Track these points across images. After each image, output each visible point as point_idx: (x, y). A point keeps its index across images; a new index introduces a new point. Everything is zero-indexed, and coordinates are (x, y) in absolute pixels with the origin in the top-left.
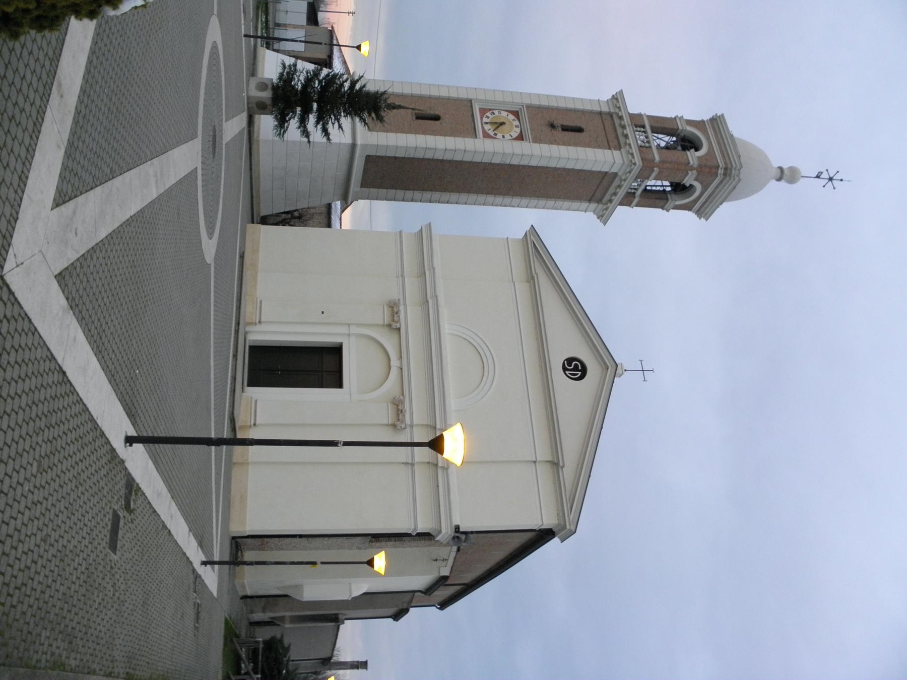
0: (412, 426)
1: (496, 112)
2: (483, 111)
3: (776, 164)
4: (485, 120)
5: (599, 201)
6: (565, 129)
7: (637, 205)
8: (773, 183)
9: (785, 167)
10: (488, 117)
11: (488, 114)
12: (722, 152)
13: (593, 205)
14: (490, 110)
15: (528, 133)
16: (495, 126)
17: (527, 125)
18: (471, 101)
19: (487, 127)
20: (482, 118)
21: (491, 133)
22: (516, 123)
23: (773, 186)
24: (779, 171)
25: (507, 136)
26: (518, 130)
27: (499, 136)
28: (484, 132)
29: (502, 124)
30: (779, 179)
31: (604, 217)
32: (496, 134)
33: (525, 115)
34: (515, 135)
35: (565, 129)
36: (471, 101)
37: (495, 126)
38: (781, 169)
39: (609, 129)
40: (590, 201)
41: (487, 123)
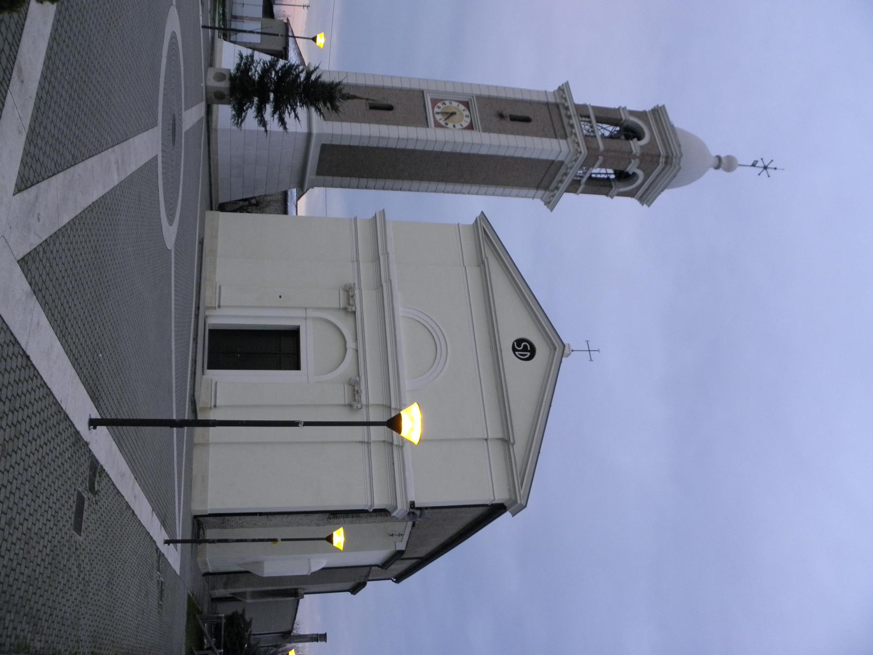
0: (367, 406)
1: (447, 103)
2: (435, 102)
3: (714, 153)
4: (436, 110)
5: (546, 188)
6: (514, 119)
7: (583, 192)
8: (712, 172)
9: (723, 155)
10: (439, 107)
11: (439, 104)
12: (663, 140)
13: (541, 192)
14: (441, 100)
15: (478, 123)
18: (423, 92)
19: (438, 117)
20: (433, 108)
21: (442, 122)
22: (467, 113)
23: (712, 175)
24: (717, 160)
25: (458, 126)
26: (469, 120)
27: (450, 125)
29: (453, 114)
30: (717, 168)
31: (551, 204)
32: (447, 124)
33: (475, 105)
34: (465, 124)
35: (514, 119)
36: (423, 92)
37: (446, 116)
39: (556, 119)
40: (538, 188)
41: (438, 113)
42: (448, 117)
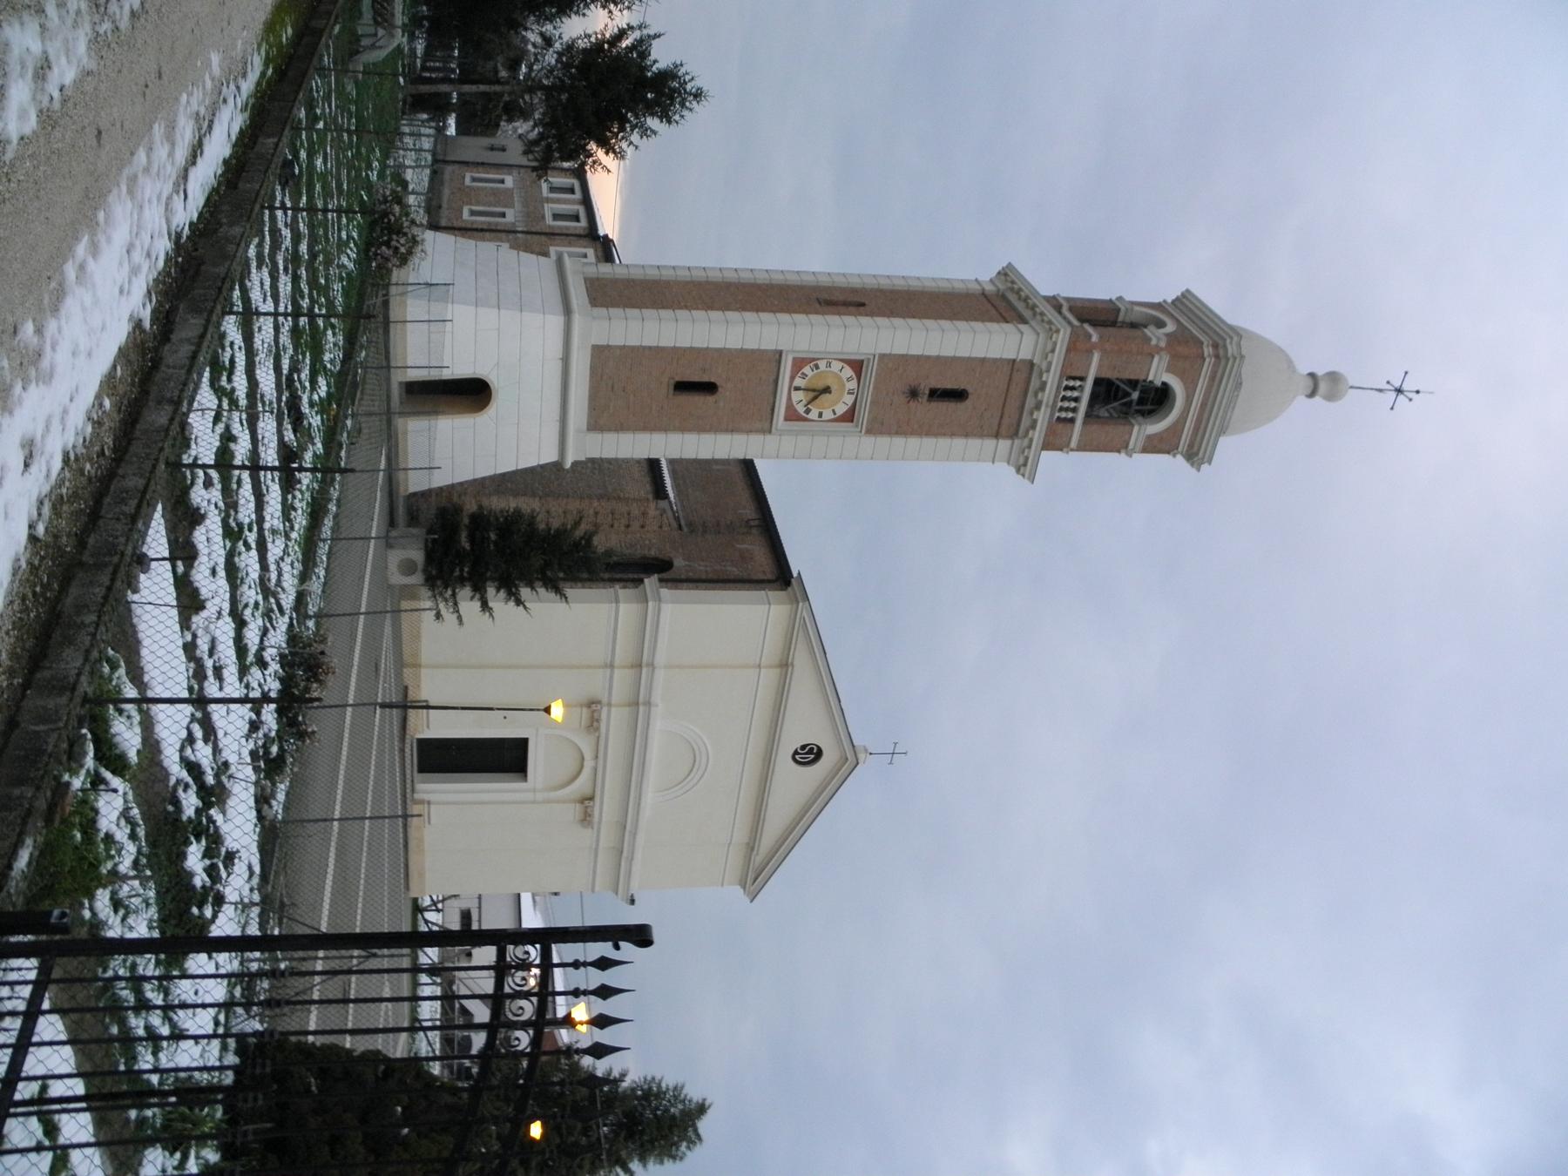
0: (609, 705)
1: (822, 364)
2: (799, 364)
3: (1304, 369)
4: (798, 382)
5: (1014, 434)
6: (939, 395)
7: (1081, 448)
8: (1302, 400)
9: (1320, 372)
10: (804, 376)
11: (807, 370)
13: (1004, 445)
15: (864, 414)
16: (811, 395)
18: (781, 353)
19: (798, 396)
20: (792, 378)
21: (801, 409)
22: (853, 385)
24: (1310, 382)
25: (828, 415)
26: (849, 400)
27: (813, 415)
28: (790, 406)
29: (827, 390)
30: (1312, 394)
31: (1024, 467)
32: (808, 411)
34: (841, 409)
35: (939, 395)
36: (781, 353)
37: (811, 395)
38: (1312, 375)
39: (1016, 391)
40: (997, 436)
41: (797, 389)
42: (815, 398)
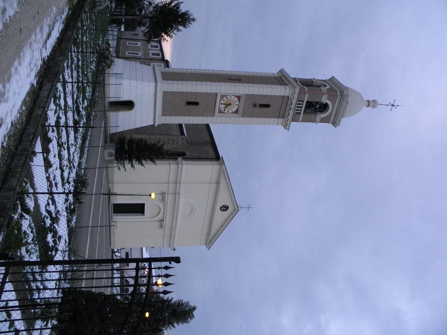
0: (168, 194)
2: (222, 97)
4: (222, 102)
5: (283, 117)
6: (262, 106)
7: (303, 121)
8: (365, 108)
9: (370, 100)
11: (224, 99)
12: (336, 113)
13: (281, 120)
14: (226, 96)
15: (241, 111)
16: (226, 106)
17: (242, 106)
18: (217, 94)
20: (220, 101)
21: (223, 110)
22: (237, 103)
23: (366, 110)
24: (367, 103)
25: (230, 111)
26: (237, 107)
27: (226, 111)
28: (219, 109)
29: (230, 104)
30: (368, 106)
31: (286, 126)
32: (225, 110)
33: (243, 99)
34: (234, 110)
35: (262, 106)
36: (217, 94)
37: (226, 106)
38: (368, 101)
39: (284, 105)
40: (278, 118)
41: (222, 104)
42: (227, 107)
